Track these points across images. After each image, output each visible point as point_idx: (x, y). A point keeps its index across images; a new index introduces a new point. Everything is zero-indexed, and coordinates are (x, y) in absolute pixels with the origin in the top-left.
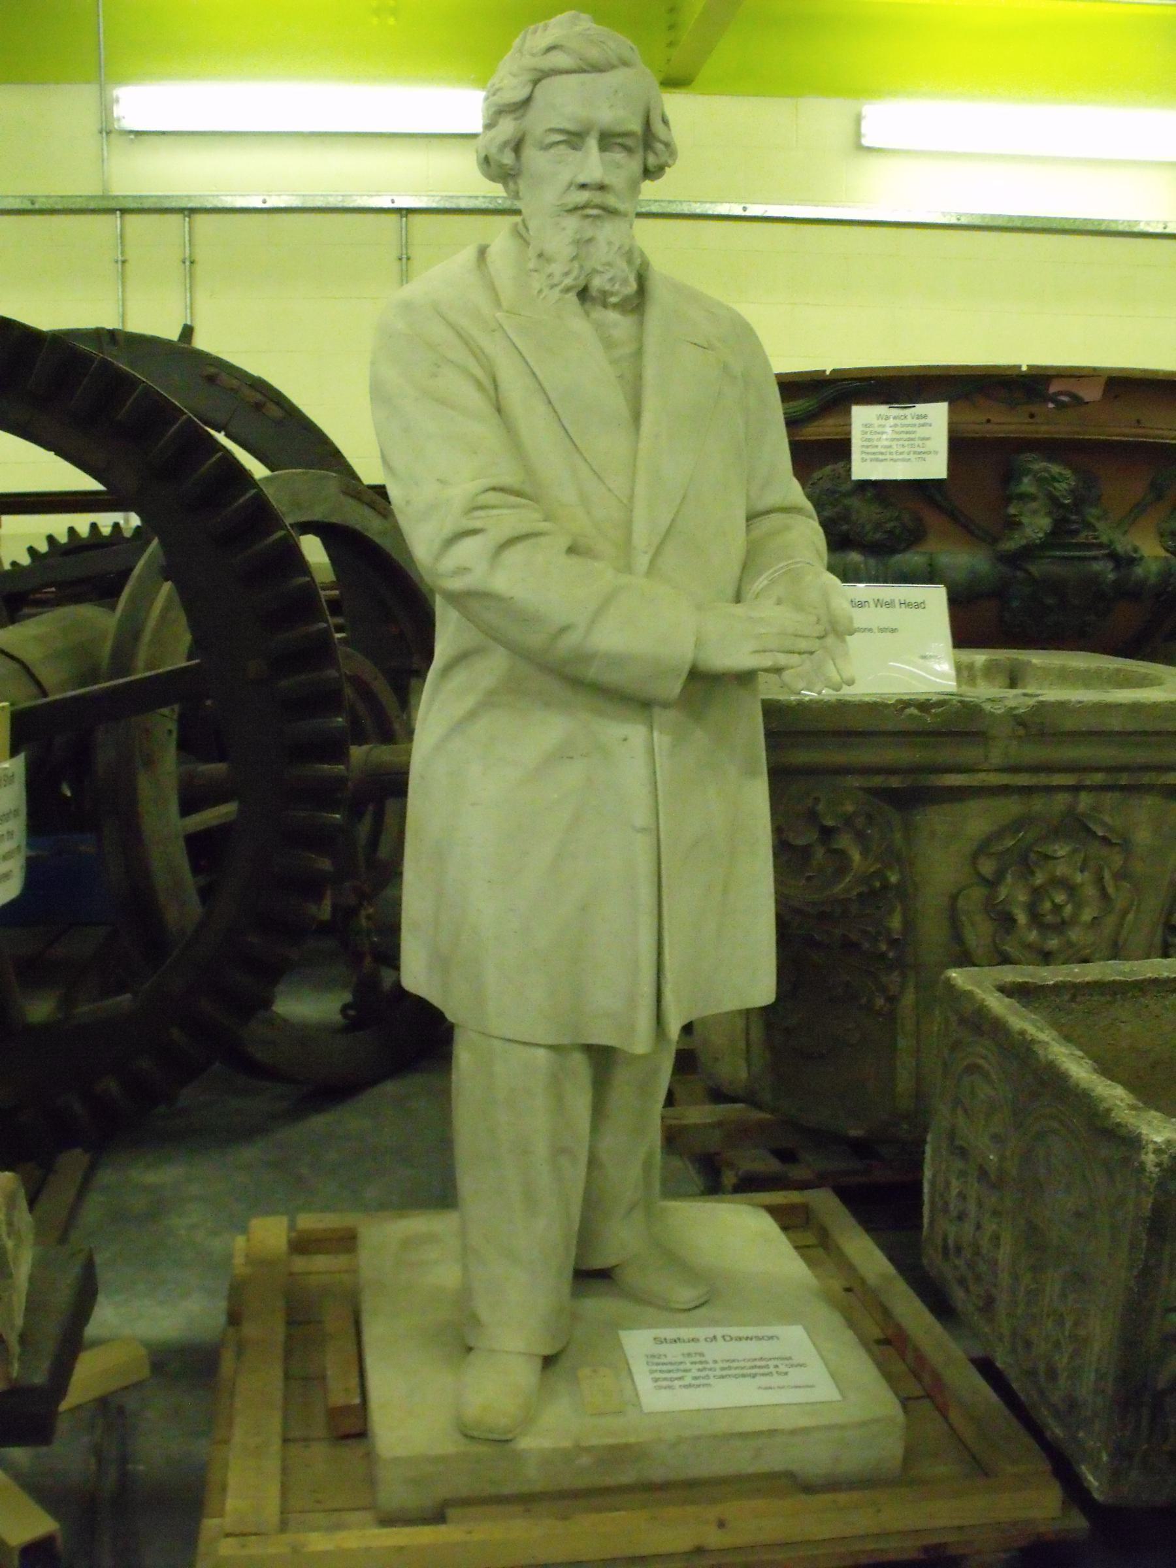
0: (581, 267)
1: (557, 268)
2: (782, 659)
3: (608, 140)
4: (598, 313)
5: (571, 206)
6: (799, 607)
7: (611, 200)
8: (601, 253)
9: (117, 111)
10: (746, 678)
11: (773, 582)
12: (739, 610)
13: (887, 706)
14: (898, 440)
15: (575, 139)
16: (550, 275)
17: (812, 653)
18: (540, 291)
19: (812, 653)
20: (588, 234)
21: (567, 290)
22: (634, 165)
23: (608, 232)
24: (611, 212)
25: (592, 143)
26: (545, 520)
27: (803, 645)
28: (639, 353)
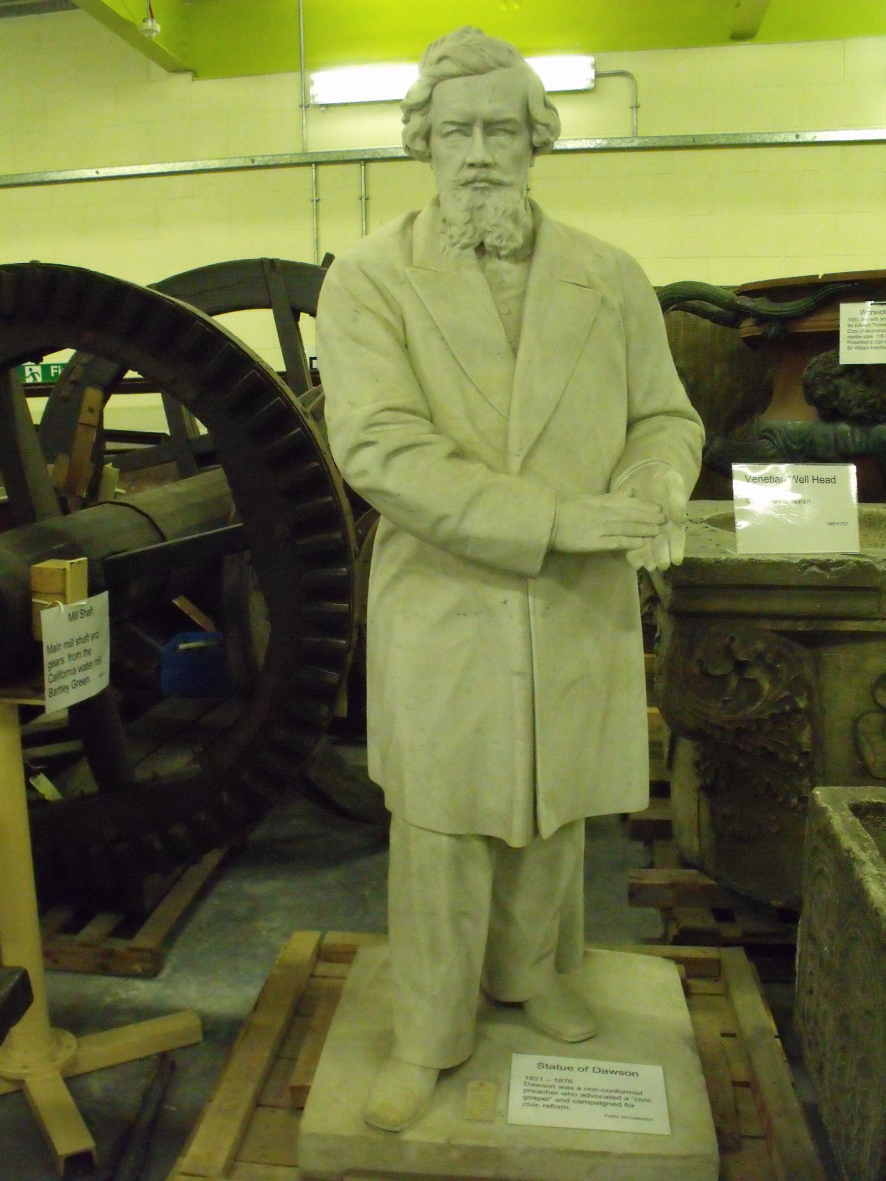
0: (475, 229)
1: (455, 231)
2: (625, 542)
3: (490, 127)
4: (493, 264)
5: (462, 182)
6: (648, 499)
7: (495, 175)
9: (313, 91)
10: (619, 554)
11: (632, 477)
12: (597, 502)
13: (790, 564)
14: (879, 331)
15: (464, 128)
16: (451, 237)
17: (653, 537)
18: (445, 249)
19: (653, 537)
20: (479, 203)
21: (465, 247)
22: (518, 144)
24: (499, 184)
25: (478, 131)
26: (434, 433)
27: (645, 530)
28: (522, 296)
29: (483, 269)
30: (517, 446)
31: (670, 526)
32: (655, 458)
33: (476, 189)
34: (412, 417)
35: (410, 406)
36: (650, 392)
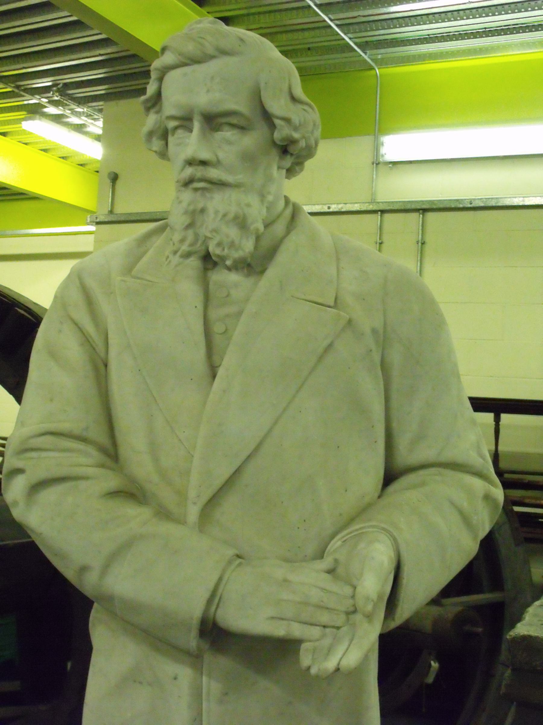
0: (196, 235)
2: (296, 631)
3: (213, 121)
7: (213, 173)
8: (210, 222)
9: (383, 150)
15: (186, 123)
18: (168, 257)
19: (338, 628)
20: (200, 206)
21: (187, 255)
23: (218, 203)
24: (222, 185)
25: (197, 125)
27: (325, 618)
30: (197, 493)
31: (358, 617)
32: (374, 523)
33: (196, 190)
34: (81, 446)
35: (77, 431)
36: (420, 438)
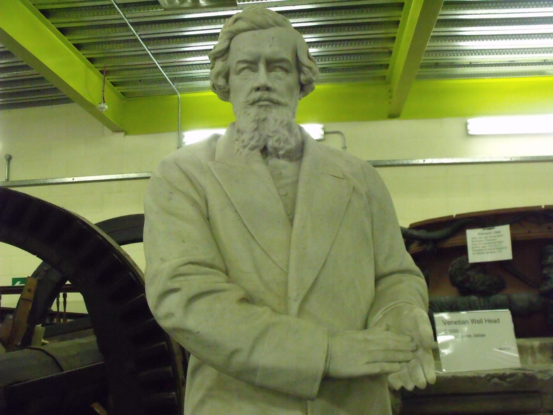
0: (261, 135)
1: (246, 137)
2: (387, 367)
3: (271, 64)
4: (274, 161)
5: (251, 102)
6: (401, 332)
7: (274, 96)
8: (271, 126)
10: (376, 378)
11: (385, 315)
12: (360, 335)
13: (479, 378)
14: (489, 243)
16: (243, 141)
17: (408, 361)
18: (238, 150)
19: (408, 361)
20: (263, 117)
21: (253, 148)
22: (291, 79)
23: (275, 114)
24: (277, 103)
25: (262, 67)
26: (228, 282)
27: (401, 356)
28: (296, 182)
29: (267, 164)
30: (295, 293)
31: (420, 352)
33: (261, 106)
35: (209, 261)
